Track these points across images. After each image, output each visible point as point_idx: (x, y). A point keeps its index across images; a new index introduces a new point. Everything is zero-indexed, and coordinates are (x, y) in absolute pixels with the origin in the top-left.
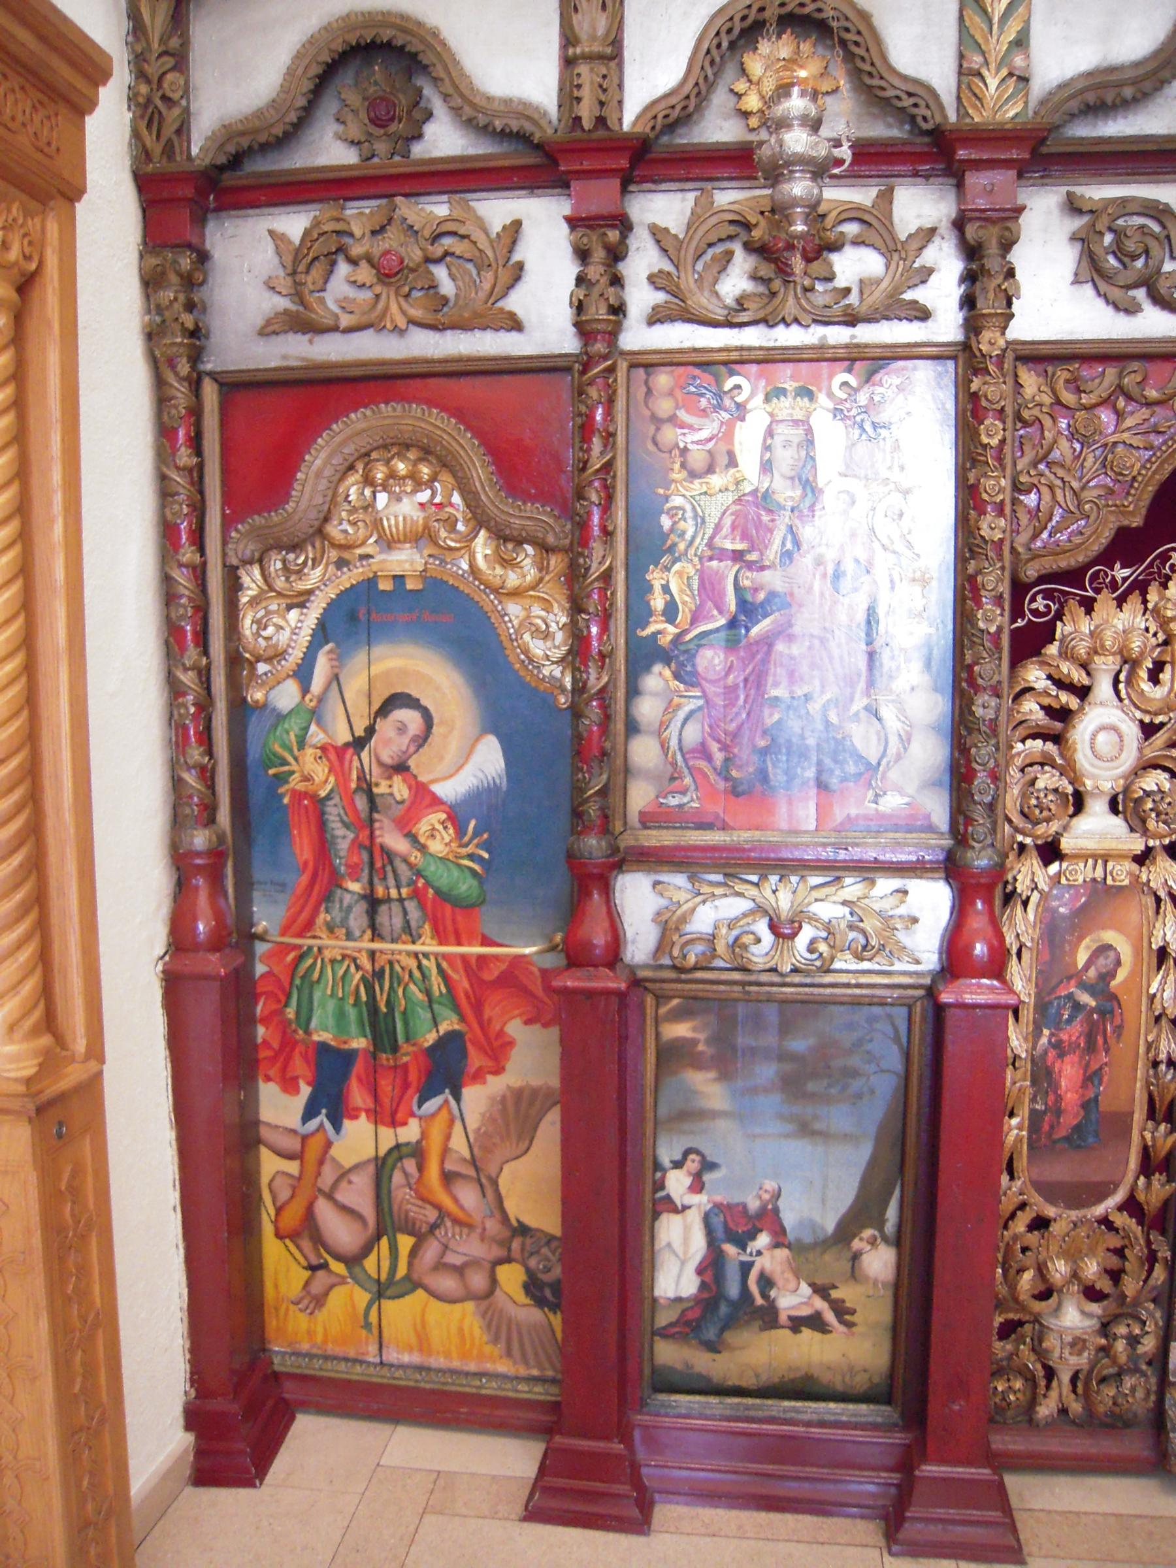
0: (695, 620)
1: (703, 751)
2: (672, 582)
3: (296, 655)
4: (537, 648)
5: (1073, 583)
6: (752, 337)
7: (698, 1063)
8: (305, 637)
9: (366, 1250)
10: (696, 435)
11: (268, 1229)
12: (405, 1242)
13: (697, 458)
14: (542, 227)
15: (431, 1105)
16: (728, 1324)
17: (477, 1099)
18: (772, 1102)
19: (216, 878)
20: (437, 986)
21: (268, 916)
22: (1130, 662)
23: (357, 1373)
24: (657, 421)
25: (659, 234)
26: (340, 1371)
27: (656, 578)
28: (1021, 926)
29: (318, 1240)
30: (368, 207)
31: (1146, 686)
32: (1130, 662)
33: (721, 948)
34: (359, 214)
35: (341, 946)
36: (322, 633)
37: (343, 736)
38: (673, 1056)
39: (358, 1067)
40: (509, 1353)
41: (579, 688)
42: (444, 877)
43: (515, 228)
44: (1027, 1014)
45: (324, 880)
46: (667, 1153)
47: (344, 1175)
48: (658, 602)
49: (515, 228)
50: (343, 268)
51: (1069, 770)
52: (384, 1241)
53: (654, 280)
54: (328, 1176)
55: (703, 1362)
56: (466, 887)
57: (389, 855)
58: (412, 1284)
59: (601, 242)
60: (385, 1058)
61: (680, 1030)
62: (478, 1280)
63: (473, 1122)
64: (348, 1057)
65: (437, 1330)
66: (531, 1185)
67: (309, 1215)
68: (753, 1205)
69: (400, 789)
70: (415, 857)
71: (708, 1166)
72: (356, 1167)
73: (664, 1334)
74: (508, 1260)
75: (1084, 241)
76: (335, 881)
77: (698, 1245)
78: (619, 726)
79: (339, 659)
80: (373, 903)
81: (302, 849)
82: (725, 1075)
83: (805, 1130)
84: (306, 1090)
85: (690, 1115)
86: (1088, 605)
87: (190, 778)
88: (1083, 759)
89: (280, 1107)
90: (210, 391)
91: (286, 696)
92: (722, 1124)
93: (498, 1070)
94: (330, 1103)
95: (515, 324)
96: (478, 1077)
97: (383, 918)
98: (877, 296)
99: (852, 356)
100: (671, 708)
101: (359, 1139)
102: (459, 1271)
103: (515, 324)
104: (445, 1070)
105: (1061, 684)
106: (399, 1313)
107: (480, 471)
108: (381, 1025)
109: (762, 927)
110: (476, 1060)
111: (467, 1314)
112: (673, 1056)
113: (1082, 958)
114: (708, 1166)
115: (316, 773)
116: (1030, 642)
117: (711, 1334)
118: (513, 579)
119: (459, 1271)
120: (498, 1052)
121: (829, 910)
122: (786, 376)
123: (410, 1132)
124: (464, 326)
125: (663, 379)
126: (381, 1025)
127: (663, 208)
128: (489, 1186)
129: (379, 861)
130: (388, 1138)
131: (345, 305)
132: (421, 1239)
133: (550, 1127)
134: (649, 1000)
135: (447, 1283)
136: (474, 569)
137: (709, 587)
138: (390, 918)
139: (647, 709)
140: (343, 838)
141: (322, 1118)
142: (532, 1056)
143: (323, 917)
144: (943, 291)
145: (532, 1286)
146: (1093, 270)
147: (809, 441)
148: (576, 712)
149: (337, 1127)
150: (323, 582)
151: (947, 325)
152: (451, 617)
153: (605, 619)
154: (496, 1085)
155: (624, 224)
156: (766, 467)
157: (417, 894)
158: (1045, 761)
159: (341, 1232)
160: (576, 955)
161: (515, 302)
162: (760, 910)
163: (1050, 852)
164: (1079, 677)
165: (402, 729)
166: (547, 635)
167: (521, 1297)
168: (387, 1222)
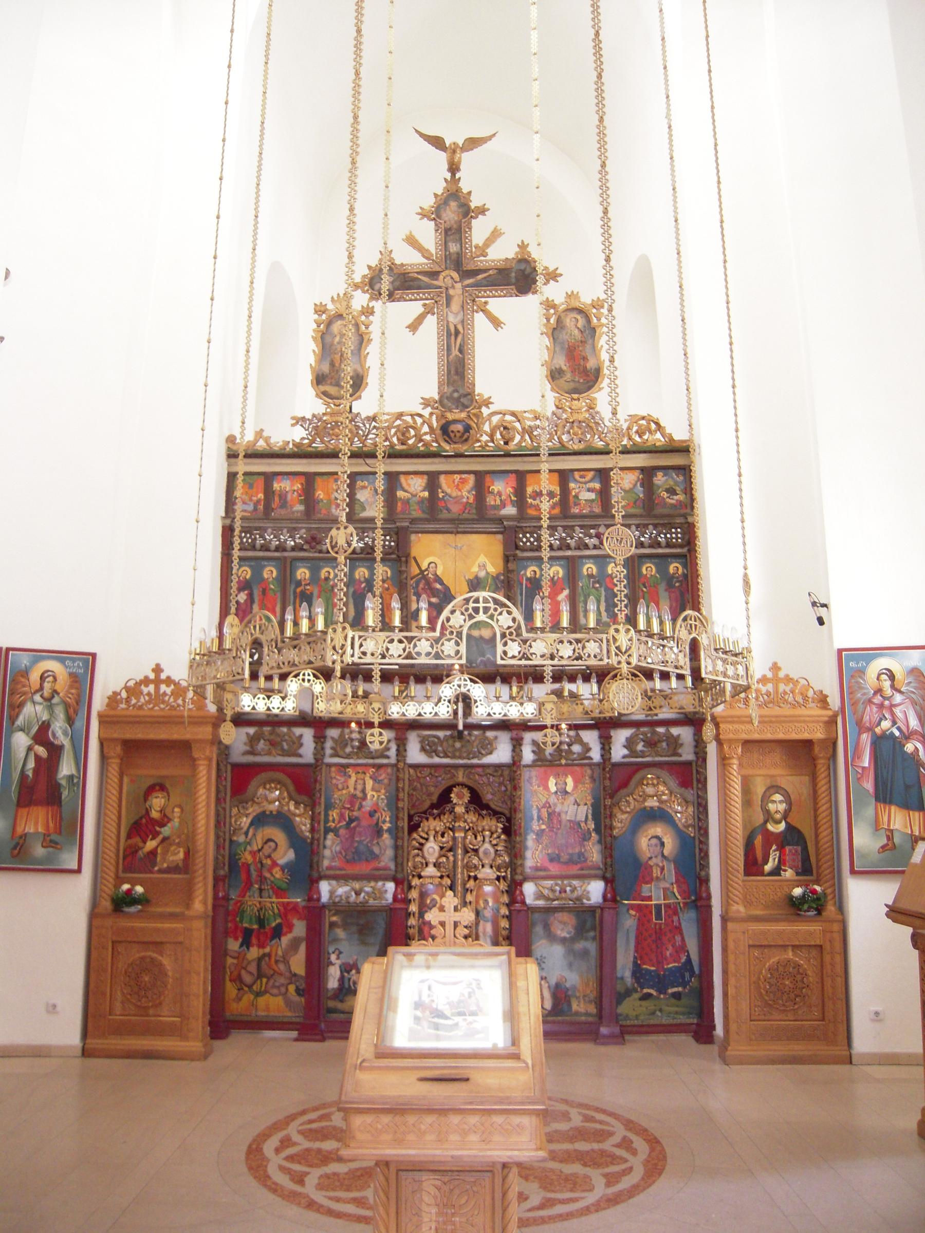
0: (339, 822)
1: (340, 853)
2: (334, 814)
3: (245, 829)
4: (303, 828)
5: (426, 814)
6: (352, 761)
7: (338, 927)
8: (247, 825)
9: (254, 983)
10: (339, 780)
11: (227, 978)
12: (264, 980)
13: (340, 786)
14: (307, 734)
15: (274, 942)
16: (346, 995)
17: (285, 940)
18: (356, 936)
19: (224, 881)
20: (276, 911)
21: (233, 895)
22: (437, 832)
23: (249, 1019)
24: (331, 778)
25: (332, 738)
26: (246, 1018)
27: (330, 813)
28: (414, 894)
29: (241, 981)
30: (269, 729)
31: (440, 838)
32: (437, 832)
33: (343, 897)
34: (267, 729)
35: (252, 901)
36: (252, 824)
37: (256, 848)
38: (332, 925)
39: (254, 934)
40: (290, 1010)
41: (313, 838)
42: (279, 884)
43: (301, 736)
44: (417, 915)
45: (248, 885)
46: (331, 950)
47: (249, 963)
48: (331, 818)
49: (301, 736)
50: (262, 741)
51: (423, 857)
52: (259, 982)
53: (332, 748)
54: (245, 962)
55: (340, 1006)
56: (284, 886)
57: (266, 878)
58: (266, 992)
59: (320, 739)
60: (262, 931)
61: (334, 919)
62: (283, 990)
63: (283, 946)
64: (252, 930)
65: (272, 1004)
66: (298, 963)
67: (239, 975)
68: (351, 962)
69: (269, 862)
70: (272, 879)
71: (341, 953)
72: (253, 960)
73: (329, 998)
74: (291, 983)
75: (421, 742)
76: (251, 885)
77: (338, 973)
78: (321, 847)
79: (256, 830)
80: (261, 890)
81: (243, 876)
82: (345, 929)
83: (363, 943)
84: (240, 940)
85: (336, 940)
86: (427, 819)
87: (220, 857)
88: (426, 854)
89: (233, 945)
90: (229, 767)
91: (242, 839)
92: (344, 943)
93: (290, 932)
94: (247, 943)
95: (300, 756)
96: (285, 934)
97: (263, 894)
98: (378, 754)
99: (374, 766)
100: (333, 843)
101: (254, 953)
102: (278, 987)
103: (300, 756)
104: (277, 933)
105: (422, 837)
106: (261, 1001)
107: (292, 788)
108: (261, 922)
109: (353, 893)
110: (285, 930)
111: (280, 1000)
112: (332, 925)
113: (428, 902)
114: (341, 953)
115: (249, 858)
116: (413, 828)
117: (341, 997)
118: (297, 811)
119: (278, 987)
120: (291, 927)
121: (367, 889)
122: (360, 769)
123: (267, 950)
124: (289, 756)
125: (333, 769)
126: (261, 922)
127: (333, 733)
128: (286, 962)
129: (262, 879)
130: (261, 951)
131: (263, 749)
132: (269, 979)
133: (303, 948)
134: (327, 912)
135: (275, 991)
136: (289, 810)
137: (342, 816)
138: (265, 894)
139: (328, 843)
140: (254, 874)
141: (245, 947)
142: (299, 928)
143: (248, 894)
144: (393, 752)
145: (297, 990)
146: (423, 749)
147: (364, 784)
148: (312, 843)
149: (248, 948)
150: (253, 810)
151: (393, 760)
152: (282, 820)
153: (319, 823)
154: (290, 936)
155: (325, 737)
156: (355, 789)
157: (272, 888)
158: (418, 855)
159: (248, 979)
160: (310, 899)
161: (301, 751)
162: (353, 889)
163: (420, 877)
164: (426, 836)
165: (270, 847)
166: (305, 825)
167: (294, 993)
168: (260, 975)
